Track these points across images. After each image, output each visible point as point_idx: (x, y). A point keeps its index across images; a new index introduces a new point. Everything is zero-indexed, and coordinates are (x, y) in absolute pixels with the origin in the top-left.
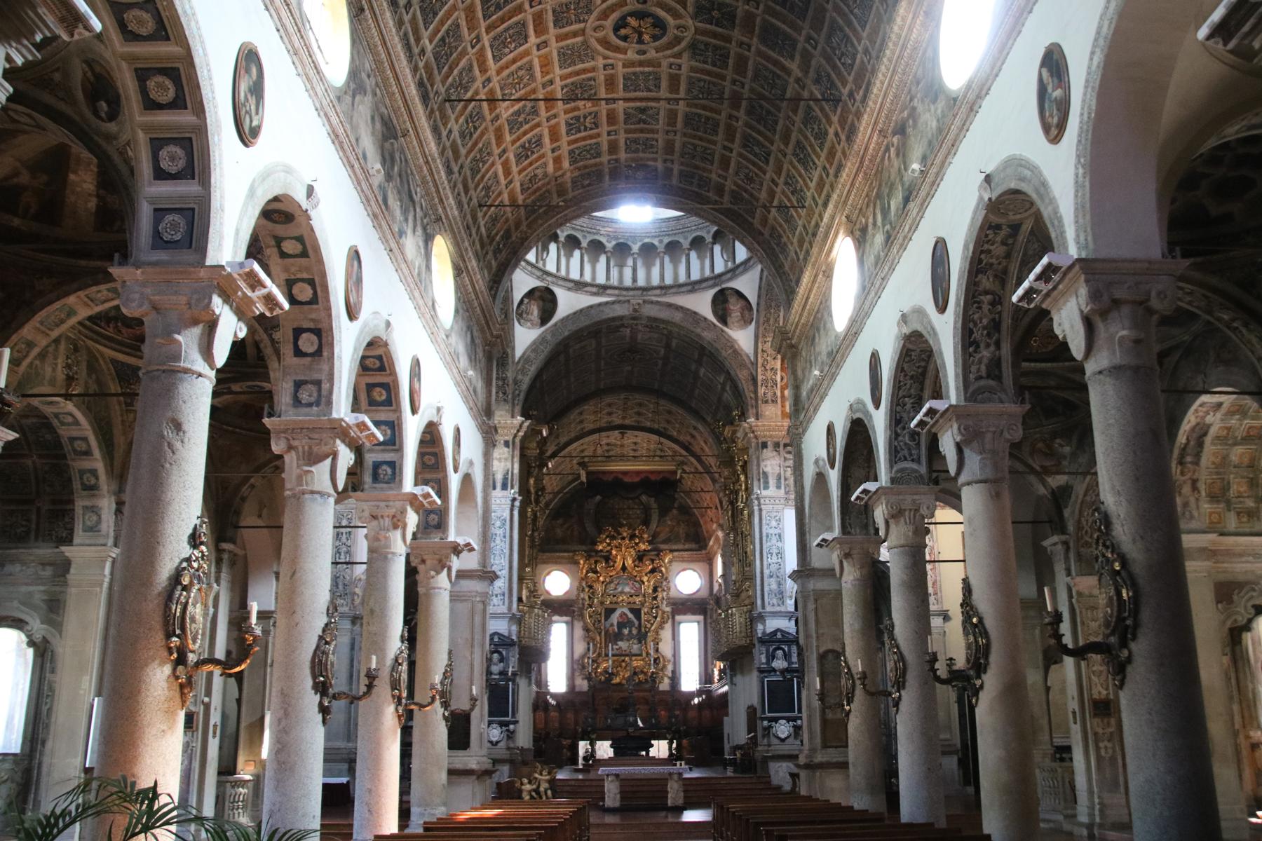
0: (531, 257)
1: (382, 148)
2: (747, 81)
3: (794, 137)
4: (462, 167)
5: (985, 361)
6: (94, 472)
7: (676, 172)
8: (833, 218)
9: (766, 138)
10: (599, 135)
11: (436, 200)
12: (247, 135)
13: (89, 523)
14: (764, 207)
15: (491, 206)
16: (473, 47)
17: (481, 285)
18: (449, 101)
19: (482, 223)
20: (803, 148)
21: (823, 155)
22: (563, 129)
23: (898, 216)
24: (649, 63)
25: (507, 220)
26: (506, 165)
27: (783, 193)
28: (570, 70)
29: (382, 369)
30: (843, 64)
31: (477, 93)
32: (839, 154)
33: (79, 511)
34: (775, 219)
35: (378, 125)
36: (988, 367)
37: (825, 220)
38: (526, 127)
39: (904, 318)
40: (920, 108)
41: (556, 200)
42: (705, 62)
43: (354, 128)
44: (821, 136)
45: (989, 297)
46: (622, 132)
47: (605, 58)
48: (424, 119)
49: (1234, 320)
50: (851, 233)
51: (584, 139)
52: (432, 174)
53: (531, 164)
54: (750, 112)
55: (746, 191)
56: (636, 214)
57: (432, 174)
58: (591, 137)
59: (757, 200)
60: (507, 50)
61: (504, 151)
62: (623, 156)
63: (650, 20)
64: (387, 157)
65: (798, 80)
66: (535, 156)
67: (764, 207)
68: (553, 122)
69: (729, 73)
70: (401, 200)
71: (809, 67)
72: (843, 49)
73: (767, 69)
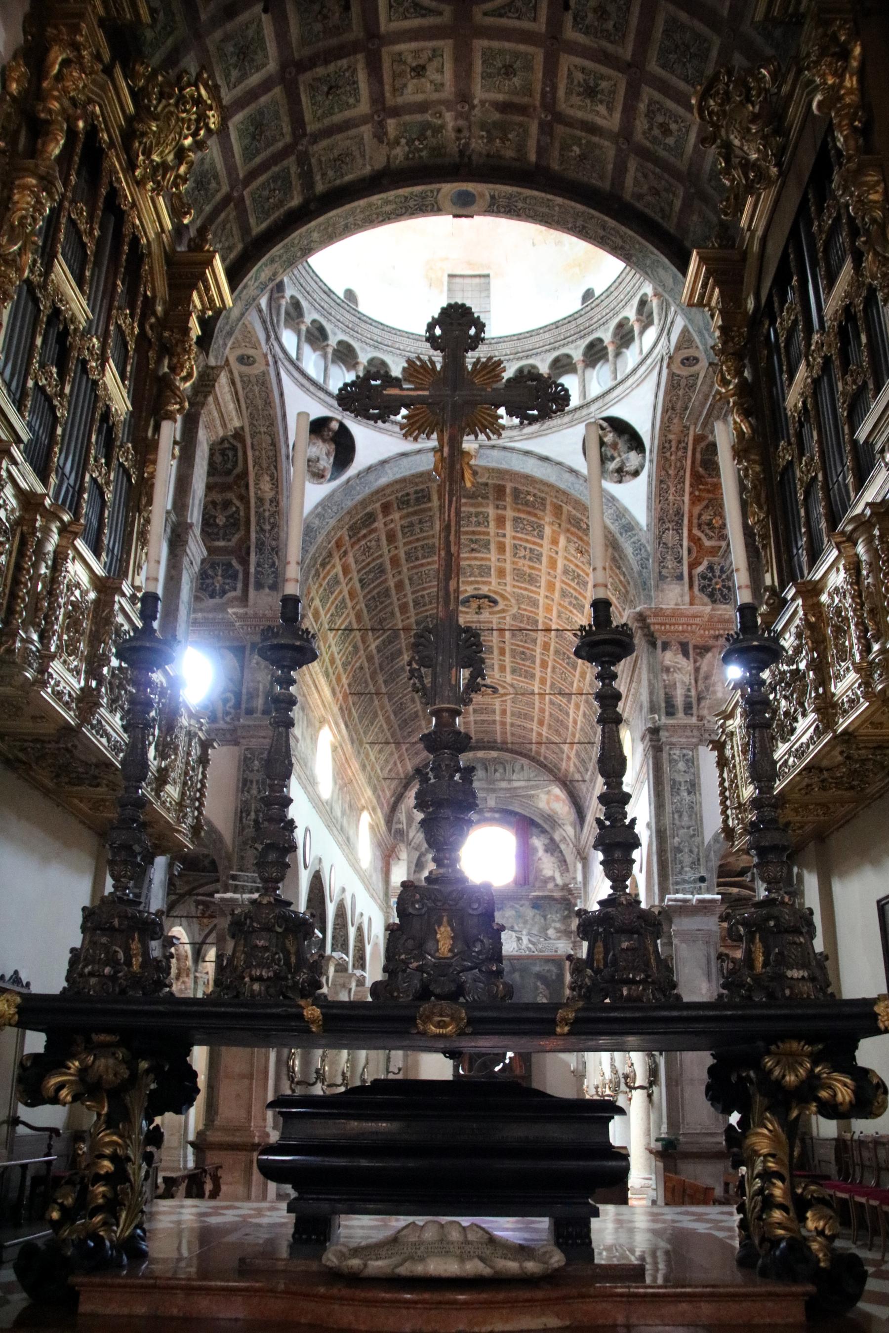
46: (492, 534)
62: (491, 511)
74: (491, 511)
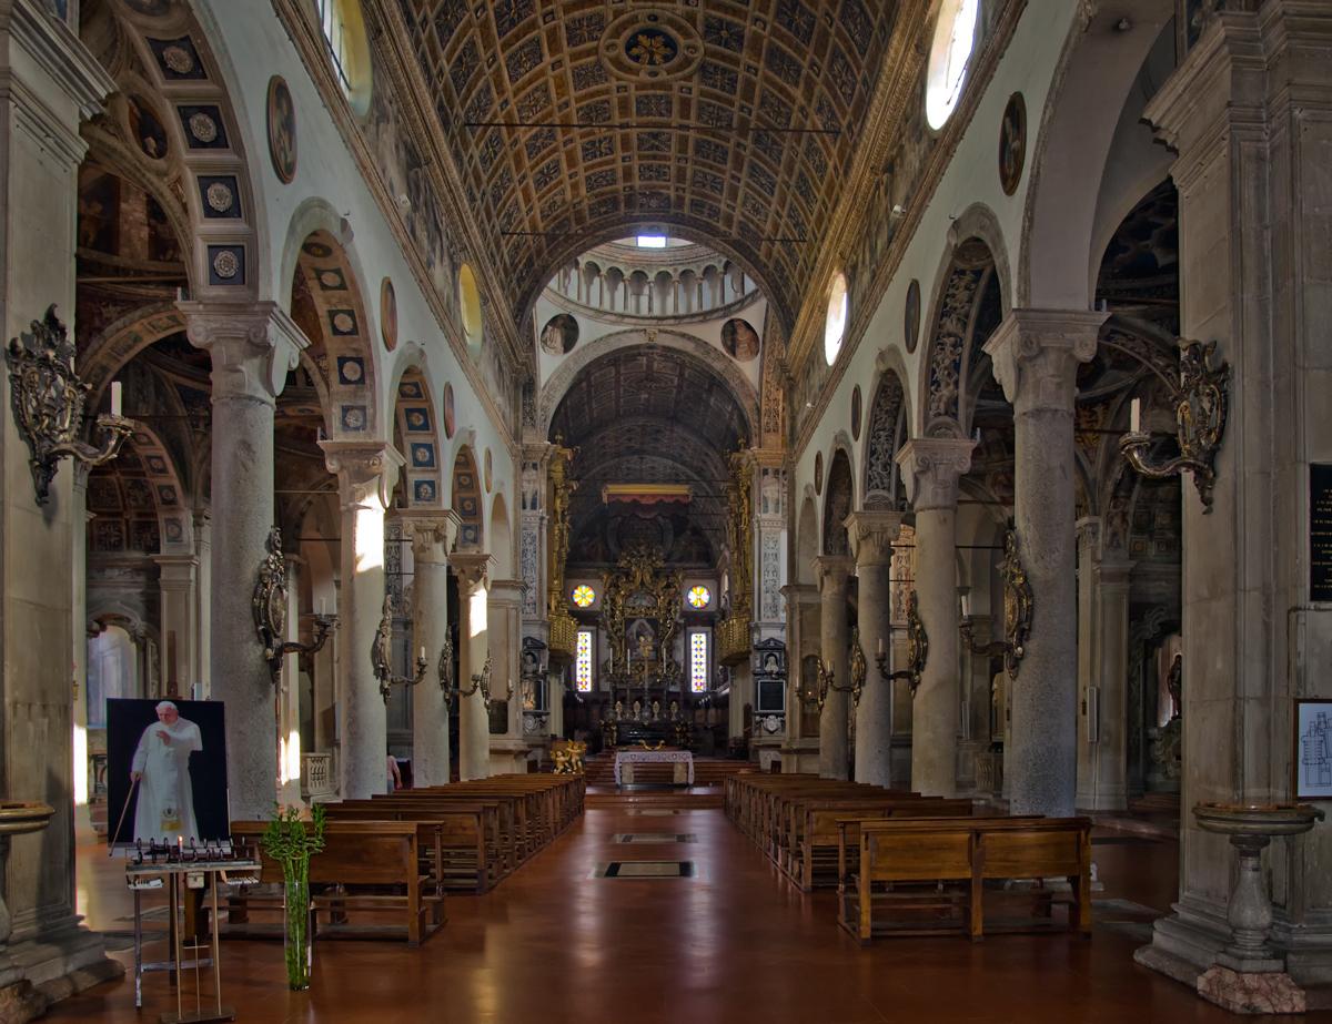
0: (553, 284)
1: (408, 177)
2: (754, 108)
3: (797, 167)
4: (484, 194)
5: (944, 399)
6: (171, 488)
7: (687, 201)
8: (828, 254)
9: (770, 167)
10: (613, 161)
11: (461, 230)
12: (285, 172)
13: (172, 534)
14: (769, 239)
15: (512, 234)
16: (489, 67)
17: (506, 314)
18: (469, 125)
19: (506, 252)
20: (806, 181)
21: (823, 188)
22: (580, 154)
23: (883, 256)
24: (661, 85)
25: (529, 247)
26: (526, 192)
27: (787, 225)
28: (584, 92)
29: (419, 395)
30: (844, 94)
31: (495, 116)
32: (837, 189)
33: (162, 524)
34: (779, 252)
35: (402, 153)
36: (947, 404)
37: (822, 256)
38: (544, 152)
39: (882, 356)
40: (907, 147)
41: (575, 228)
42: (715, 86)
43: (381, 159)
44: (822, 168)
45: (952, 339)
47: (618, 79)
48: (445, 146)
49: (1168, 366)
50: (844, 271)
51: (600, 164)
52: (456, 203)
53: (550, 190)
54: (757, 141)
55: (752, 222)
56: (652, 242)
57: (456, 203)
58: (607, 163)
59: (763, 232)
60: (522, 70)
61: (524, 177)
62: (637, 183)
63: (660, 39)
64: (413, 186)
65: (802, 109)
66: (554, 182)
67: (769, 239)
68: (569, 146)
69: (737, 99)
70: (428, 231)
71: (812, 95)
72: (844, 78)
73: (773, 95)
74: (637, 183)
